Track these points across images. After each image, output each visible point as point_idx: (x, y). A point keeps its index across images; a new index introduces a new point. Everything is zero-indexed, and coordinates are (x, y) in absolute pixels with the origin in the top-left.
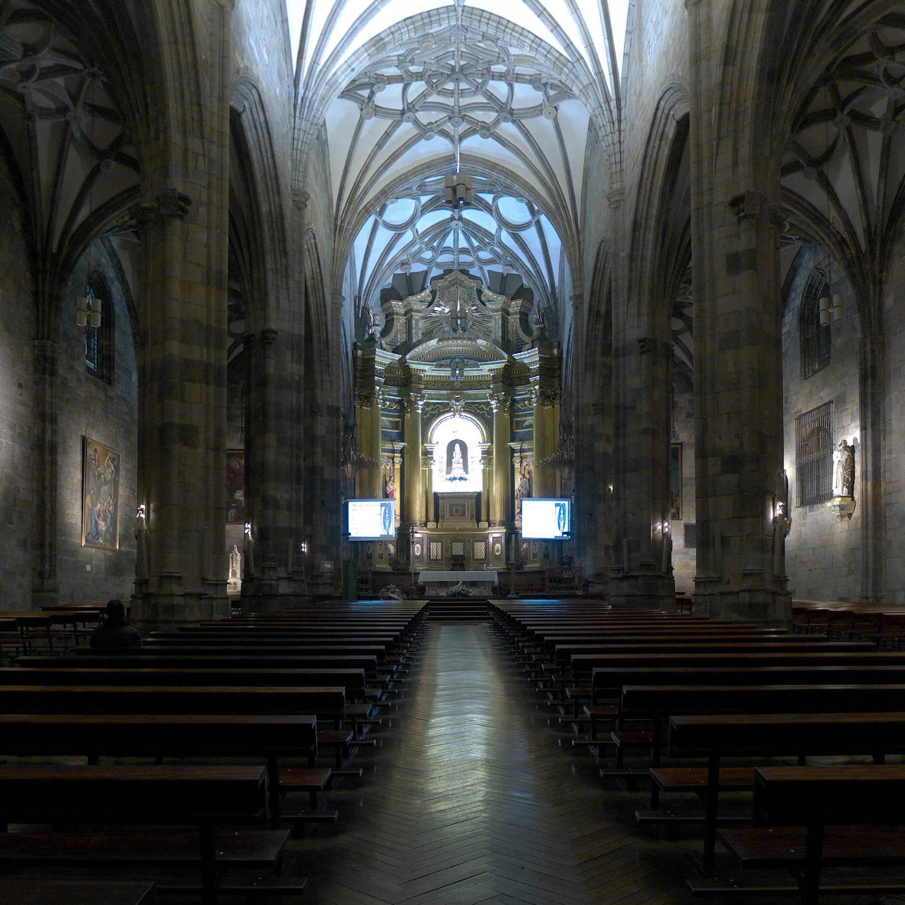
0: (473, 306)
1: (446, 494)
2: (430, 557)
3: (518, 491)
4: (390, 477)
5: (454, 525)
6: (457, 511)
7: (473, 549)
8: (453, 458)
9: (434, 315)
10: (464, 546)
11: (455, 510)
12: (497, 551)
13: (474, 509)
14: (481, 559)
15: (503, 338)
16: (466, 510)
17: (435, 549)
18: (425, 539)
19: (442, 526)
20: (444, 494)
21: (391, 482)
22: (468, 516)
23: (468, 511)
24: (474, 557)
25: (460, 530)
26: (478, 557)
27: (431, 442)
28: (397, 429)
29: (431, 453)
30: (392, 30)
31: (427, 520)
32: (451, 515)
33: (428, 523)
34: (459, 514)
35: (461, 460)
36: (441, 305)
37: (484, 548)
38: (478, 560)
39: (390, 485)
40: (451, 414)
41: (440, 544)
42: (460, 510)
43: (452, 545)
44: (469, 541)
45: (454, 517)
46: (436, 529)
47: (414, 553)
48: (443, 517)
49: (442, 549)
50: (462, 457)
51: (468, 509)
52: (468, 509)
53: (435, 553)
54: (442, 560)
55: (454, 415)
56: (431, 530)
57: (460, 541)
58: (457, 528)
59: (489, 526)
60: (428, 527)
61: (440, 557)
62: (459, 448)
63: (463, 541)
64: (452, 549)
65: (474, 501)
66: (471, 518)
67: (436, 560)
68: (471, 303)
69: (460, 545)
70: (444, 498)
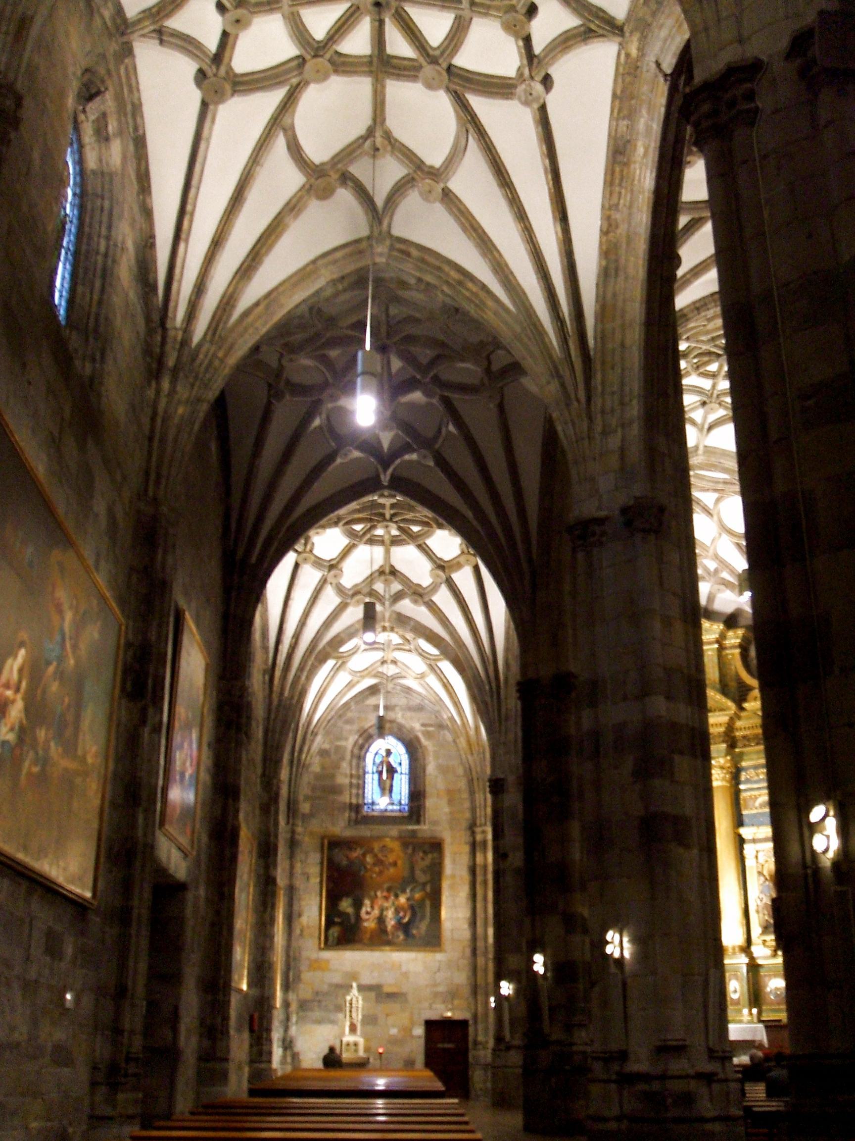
12: (735, 991)
15: (721, 681)
30: (698, 305)
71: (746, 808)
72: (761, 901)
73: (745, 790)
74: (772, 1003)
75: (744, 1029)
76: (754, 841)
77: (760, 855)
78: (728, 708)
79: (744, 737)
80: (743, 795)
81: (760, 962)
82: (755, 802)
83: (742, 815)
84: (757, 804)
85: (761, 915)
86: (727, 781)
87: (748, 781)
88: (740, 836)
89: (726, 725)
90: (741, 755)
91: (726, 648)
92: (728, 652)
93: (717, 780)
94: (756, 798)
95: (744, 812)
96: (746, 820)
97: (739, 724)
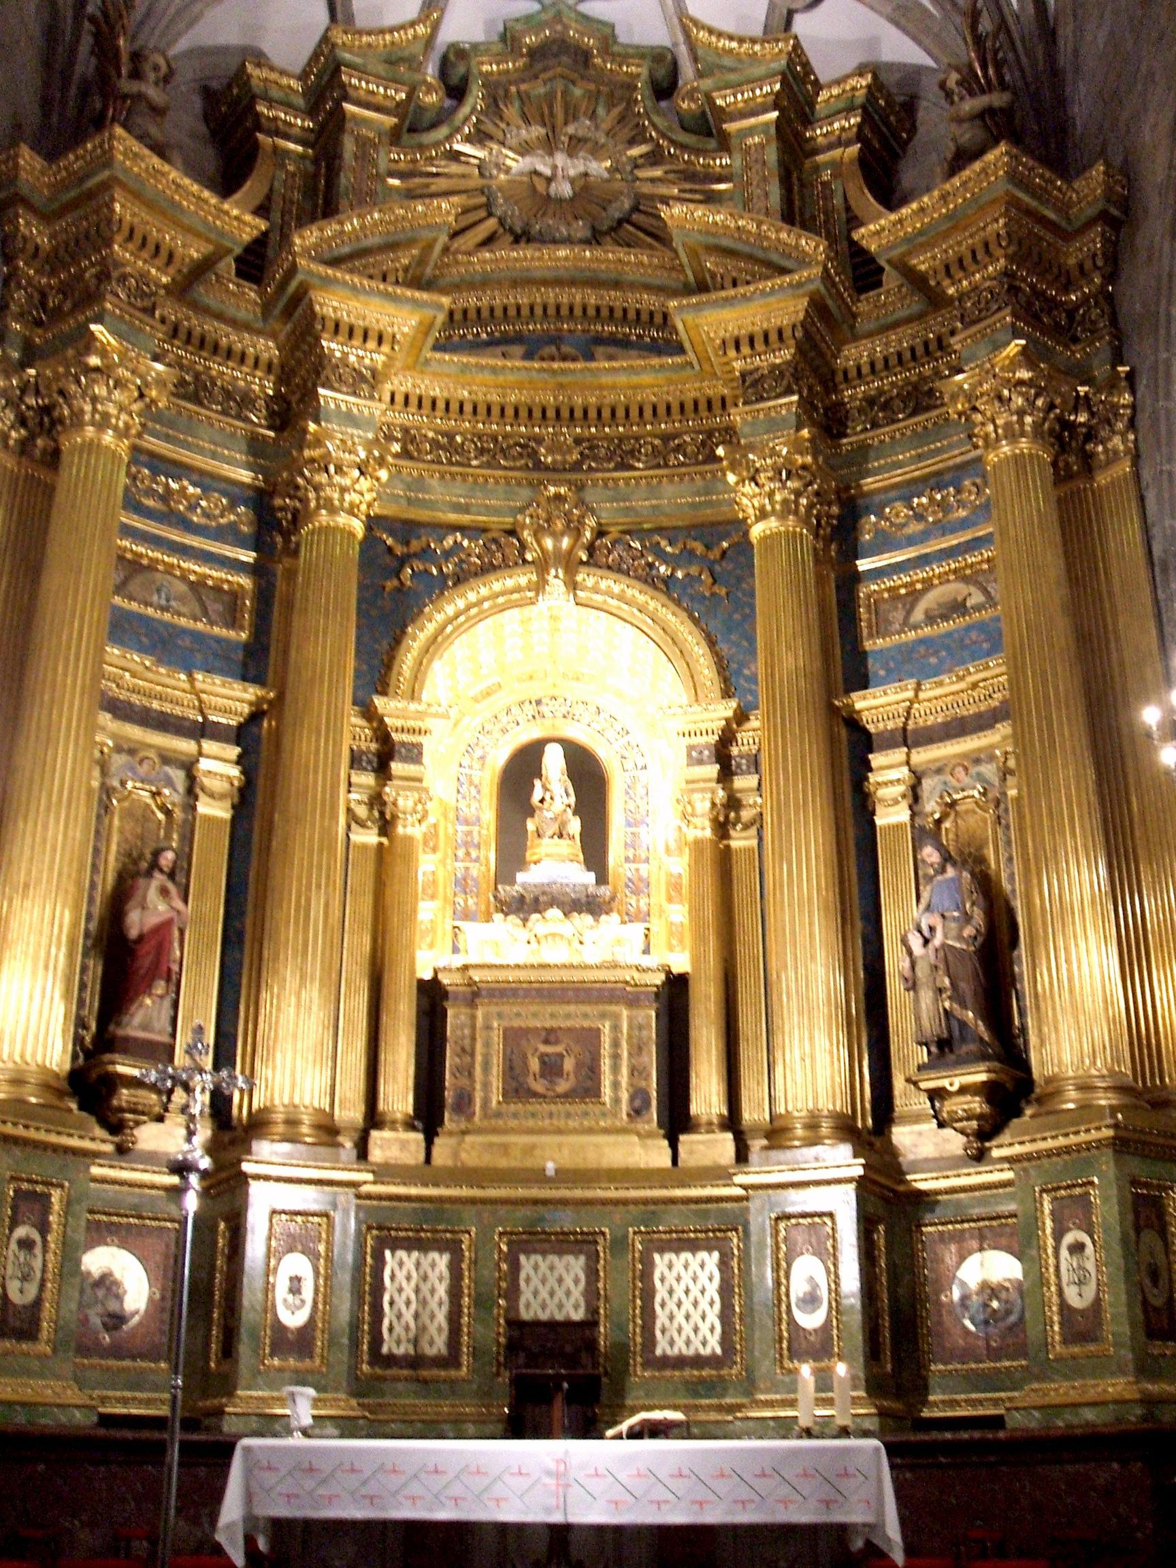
0: (632, 142)
1: (489, 975)
2: (377, 1340)
3: (915, 942)
4: (157, 853)
5: (529, 1150)
6: (551, 1068)
7: (648, 1294)
8: (530, 811)
9: (454, 168)
10: (592, 1273)
11: (534, 1064)
12: (811, 1301)
13: (651, 1060)
14: (698, 1361)
16: (606, 1065)
17: (409, 1291)
18: (347, 1224)
19: (456, 1155)
20: (477, 976)
21: (159, 879)
22: (617, 1101)
23: (615, 1069)
24: (650, 1342)
25: (566, 1176)
26: (680, 1348)
27: (413, 696)
28: (232, 621)
29: (414, 754)
31: (374, 1118)
32: (516, 1089)
33: (375, 1134)
34: (563, 1086)
35: (575, 825)
36: (491, 138)
37: (713, 1289)
38: (680, 1362)
39: (152, 894)
40: (523, 578)
41: (442, 1261)
42: (569, 1064)
43: (515, 1267)
44: (620, 1244)
45: (534, 1106)
46: (426, 1170)
47: (269, 1307)
48: (464, 1104)
49: (455, 1293)
50: (579, 810)
51: (616, 1057)
52: (616, 1057)
53: (408, 1316)
54: (451, 1359)
55: (539, 587)
56: (384, 1173)
57: (564, 1243)
58: (550, 1167)
59: (742, 1156)
60: (376, 1154)
61: (438, 1344)
62: (562, 764)
63: (583, 1243)
64: (513, 1293)
65: (649, 1015)
66: (637, 1112)
67: (416, 1361)
68: (626, 133)
69: (573, 1267)
70: (474, 995)
71: (880, 629)
72: (926, 942)
73: (878, 573)
74: (965, 1355)
75: (773, 1468)
76: (906, 738)
77: (927, 784)
78: (804, 261)
79: (871, 401)
80: (866, 589)
81: (923, 1182)
82: (909, 613)
83: (864, 654)
84: (918, 615)
85: (926, 996)
86: (806, 522)
87: (884, 544)
88: (853, 723)
89: (799, 334)
90: (863, 450)
91: (816, 151)
92: (821, 158)
93: (763, 515)
94: (914, 596)
95: (868, 645)
96: (874, 667)
97: (854, 355)
